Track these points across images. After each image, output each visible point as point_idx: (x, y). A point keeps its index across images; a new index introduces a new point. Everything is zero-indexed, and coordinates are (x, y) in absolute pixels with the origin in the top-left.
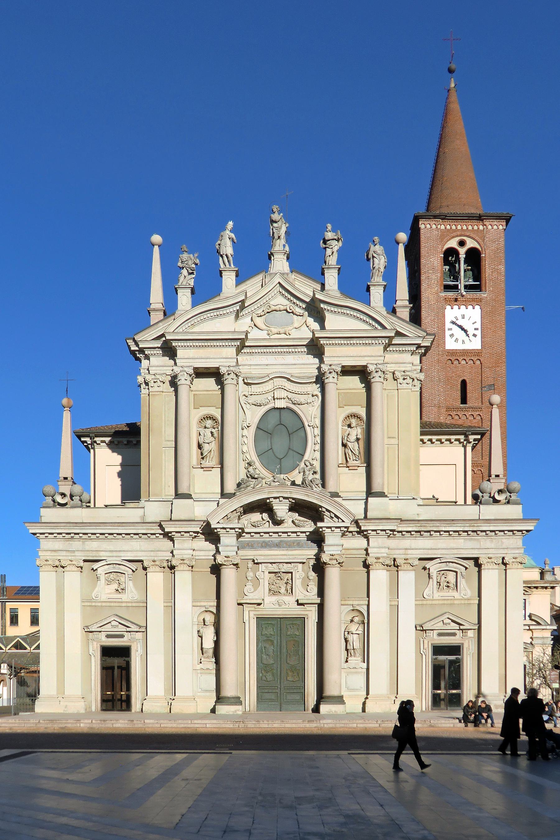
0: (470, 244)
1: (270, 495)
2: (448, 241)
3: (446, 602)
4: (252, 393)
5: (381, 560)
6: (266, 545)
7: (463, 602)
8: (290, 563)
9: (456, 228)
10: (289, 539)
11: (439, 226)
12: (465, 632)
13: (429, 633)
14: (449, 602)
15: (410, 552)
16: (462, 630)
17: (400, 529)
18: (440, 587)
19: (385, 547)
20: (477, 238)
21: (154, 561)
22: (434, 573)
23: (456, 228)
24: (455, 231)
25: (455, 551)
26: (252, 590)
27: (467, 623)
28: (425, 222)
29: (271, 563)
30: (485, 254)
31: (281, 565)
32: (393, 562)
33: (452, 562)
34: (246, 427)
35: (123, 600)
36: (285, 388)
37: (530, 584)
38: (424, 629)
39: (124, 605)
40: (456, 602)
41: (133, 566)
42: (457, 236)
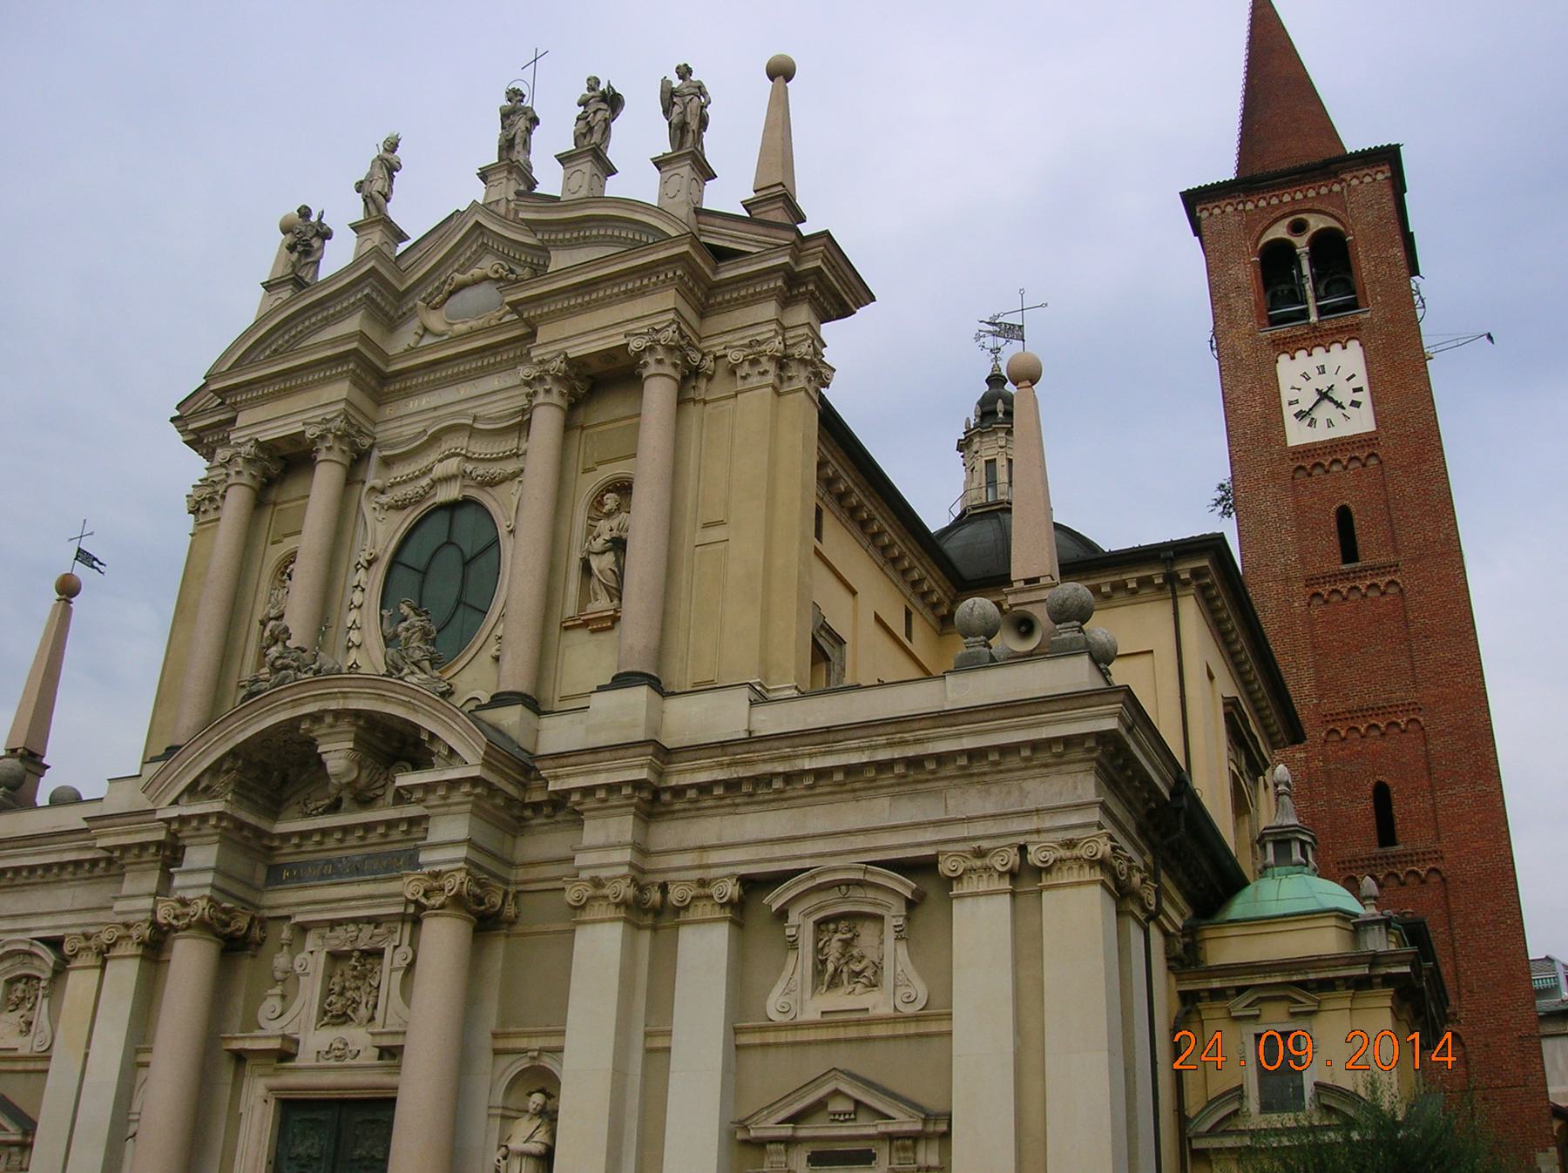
0: (1316, 223)
1: (296, 709)
2: (1266, 229)
3: (841, 1033)
4: (392, 480)
5: (606, 891)
6: (335, 871)
7: (901, 1029)
8: (375, 921)
9: (1281, 201)
10: (388, 848)
11: (1241, 207)
12: (905, 1149)
13: (778, 1153)
14: (853, 1032)
15: (714, 857)
16: (890, 1137)
17: (674, 781)
18: (827, 977)
19: (620, 846)
20: (1330, 209)
21: (87, 937)
22: (801, 923)
23: (1281, 201)
24: (1277, 207)
25: (859, 842)
26: (278, 1012)
27: (901, 1110)
28: (1210, 206)
29: (334, 924)
30: (1353, 235)
31: (352, 927)
32: (655, 896)
33: (859, 884)
34: (365, 564)
35: (21, 1052)
36: (463, 452)
37: (1298, 971)
38: (752, 1133)
39: (19, 1066)
40: (877, 1031)
41: (49, 957)
42: (1284, 216)
